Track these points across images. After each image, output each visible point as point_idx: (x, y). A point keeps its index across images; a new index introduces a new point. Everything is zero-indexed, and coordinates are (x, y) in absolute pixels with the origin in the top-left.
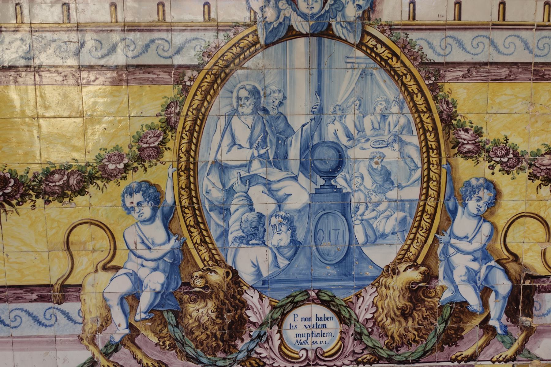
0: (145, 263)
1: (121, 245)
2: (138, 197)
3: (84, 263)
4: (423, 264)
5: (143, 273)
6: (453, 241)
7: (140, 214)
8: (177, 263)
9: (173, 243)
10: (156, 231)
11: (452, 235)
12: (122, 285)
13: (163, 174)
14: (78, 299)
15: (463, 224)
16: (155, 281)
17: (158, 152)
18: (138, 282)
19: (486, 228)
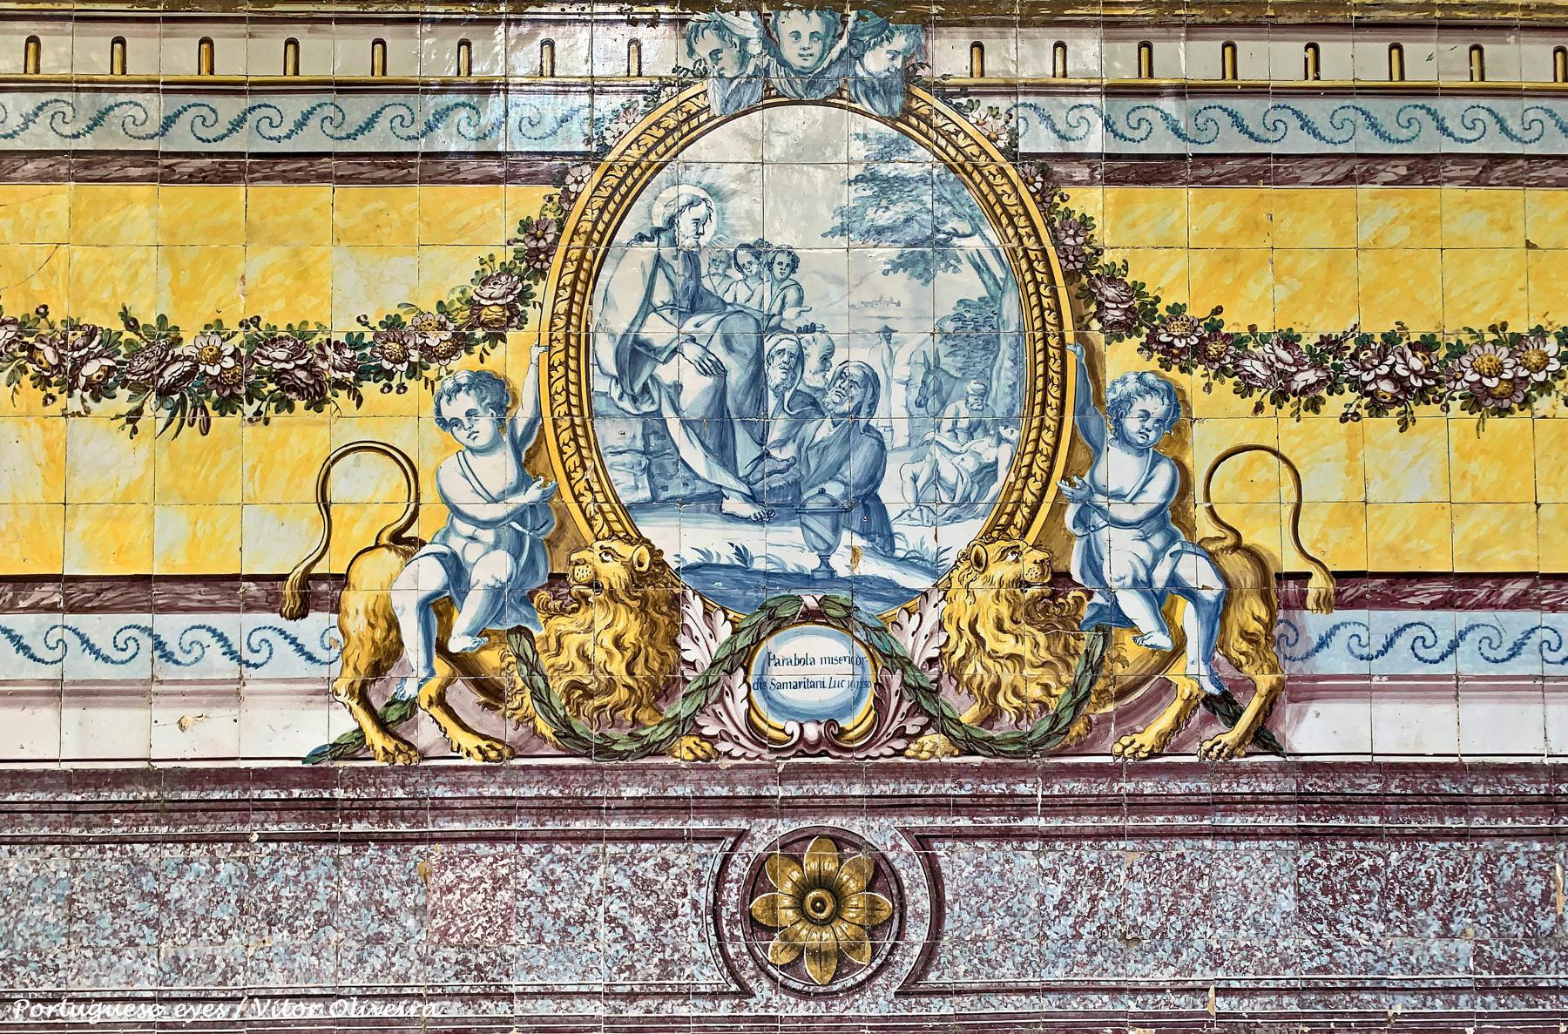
0: (480, 533)
1: (428, 493)
2: (466, 401)
3: (354, 531)
4: (1034, 547)
5: (471, 554)
6: (1099, 499)
7: (473, 435)
8: (537, 533)
9: (533, 494)
10: (499, 469)
11: (1095, 488)
12: (431, 576)
13: (518, 358)
14: (336, 607)
15: (1119, 468)
16: (491, 568)
17: (513, 316)
18: (456, 569)
19: (1164, 472)
